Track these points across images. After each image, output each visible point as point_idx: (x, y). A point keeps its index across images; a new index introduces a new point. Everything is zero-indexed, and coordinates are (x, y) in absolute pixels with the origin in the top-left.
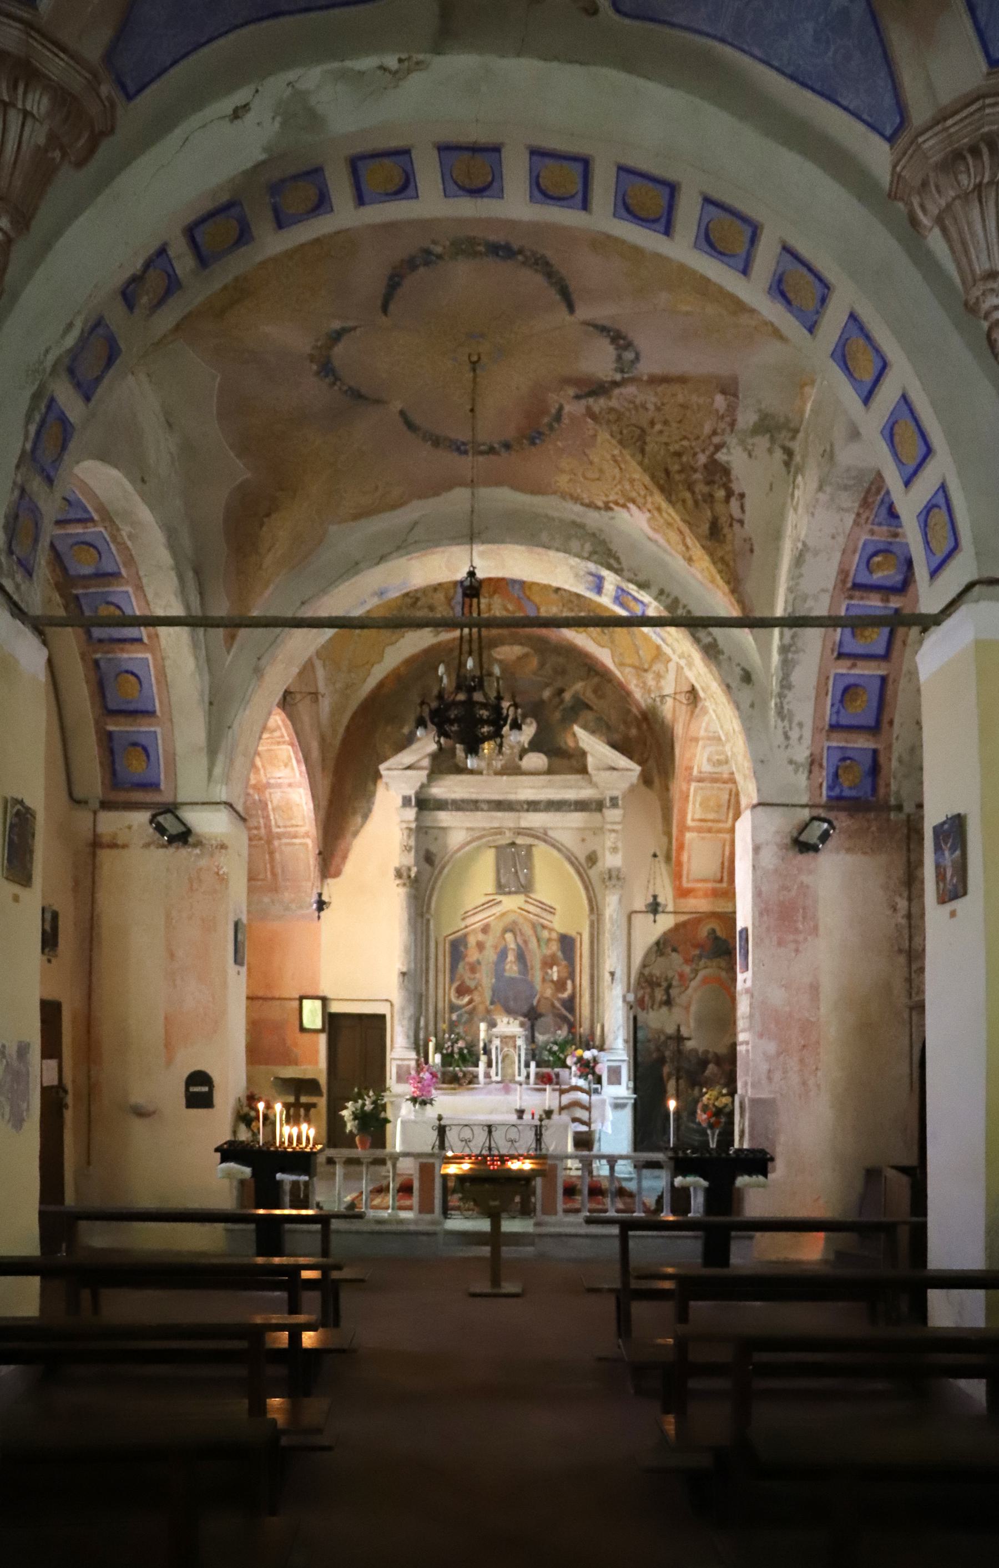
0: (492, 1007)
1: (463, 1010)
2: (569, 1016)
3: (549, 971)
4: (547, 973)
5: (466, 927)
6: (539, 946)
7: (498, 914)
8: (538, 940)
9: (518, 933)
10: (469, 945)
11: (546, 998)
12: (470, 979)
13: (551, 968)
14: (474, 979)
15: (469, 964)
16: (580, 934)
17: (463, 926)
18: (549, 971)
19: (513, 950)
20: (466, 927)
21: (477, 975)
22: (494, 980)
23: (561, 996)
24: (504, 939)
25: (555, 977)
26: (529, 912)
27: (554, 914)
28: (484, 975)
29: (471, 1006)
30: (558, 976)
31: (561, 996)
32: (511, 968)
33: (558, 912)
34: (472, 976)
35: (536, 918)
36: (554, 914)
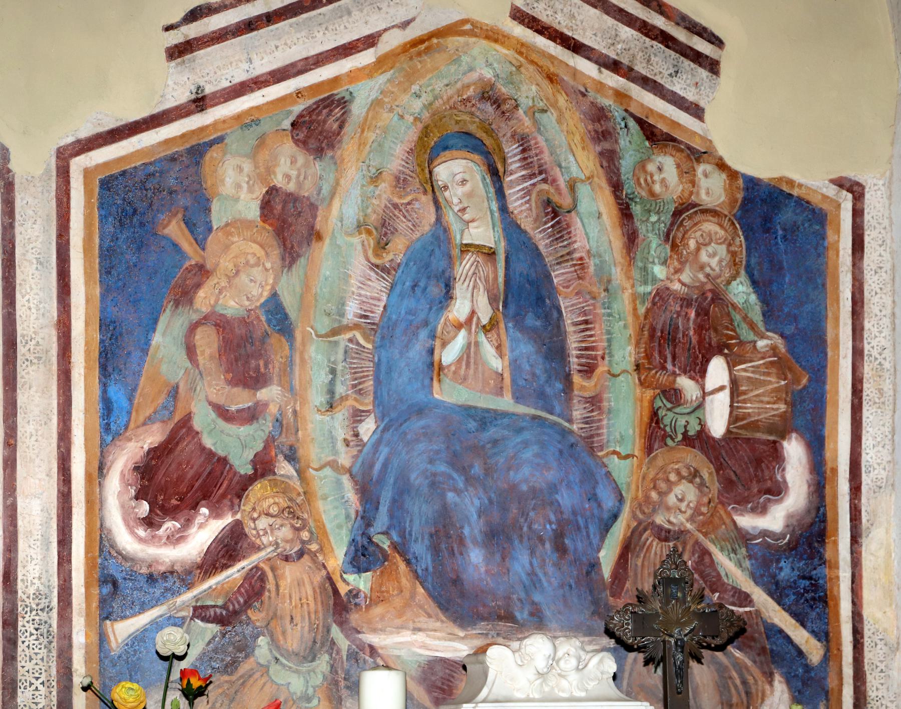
0: (362, 582)
1: (187, 597)
2: (800, 636)
3: (685, 383)
4: (673, 395)
5: (200, 103)
6: (631, 239)
7: (392, 41)
8: (625, 213)
9: (512, 150)
10: (219, 216)
11: (664, 535)
12: (223, 413)
13: (699, 371)
14: (251, 415)
15: (221, 323)
16: (856, 191)
17: (181, 96)
18: (685, 383)
19: (491, 254)
20: (200, 103)
21: (270, 394)
22: (368, 428)
23: (747, 521)
24: (431, 187)
25: (718, 426)
26: (577, 47)
27: (713, 67)
28: (317, 398)
29: (235, 573)
30: (734, 418)
31: (747, 521)
32: (470, 353)
33: (728, 59)
34: (241, 399)
35: (613, 80)
36: (713, 67)
